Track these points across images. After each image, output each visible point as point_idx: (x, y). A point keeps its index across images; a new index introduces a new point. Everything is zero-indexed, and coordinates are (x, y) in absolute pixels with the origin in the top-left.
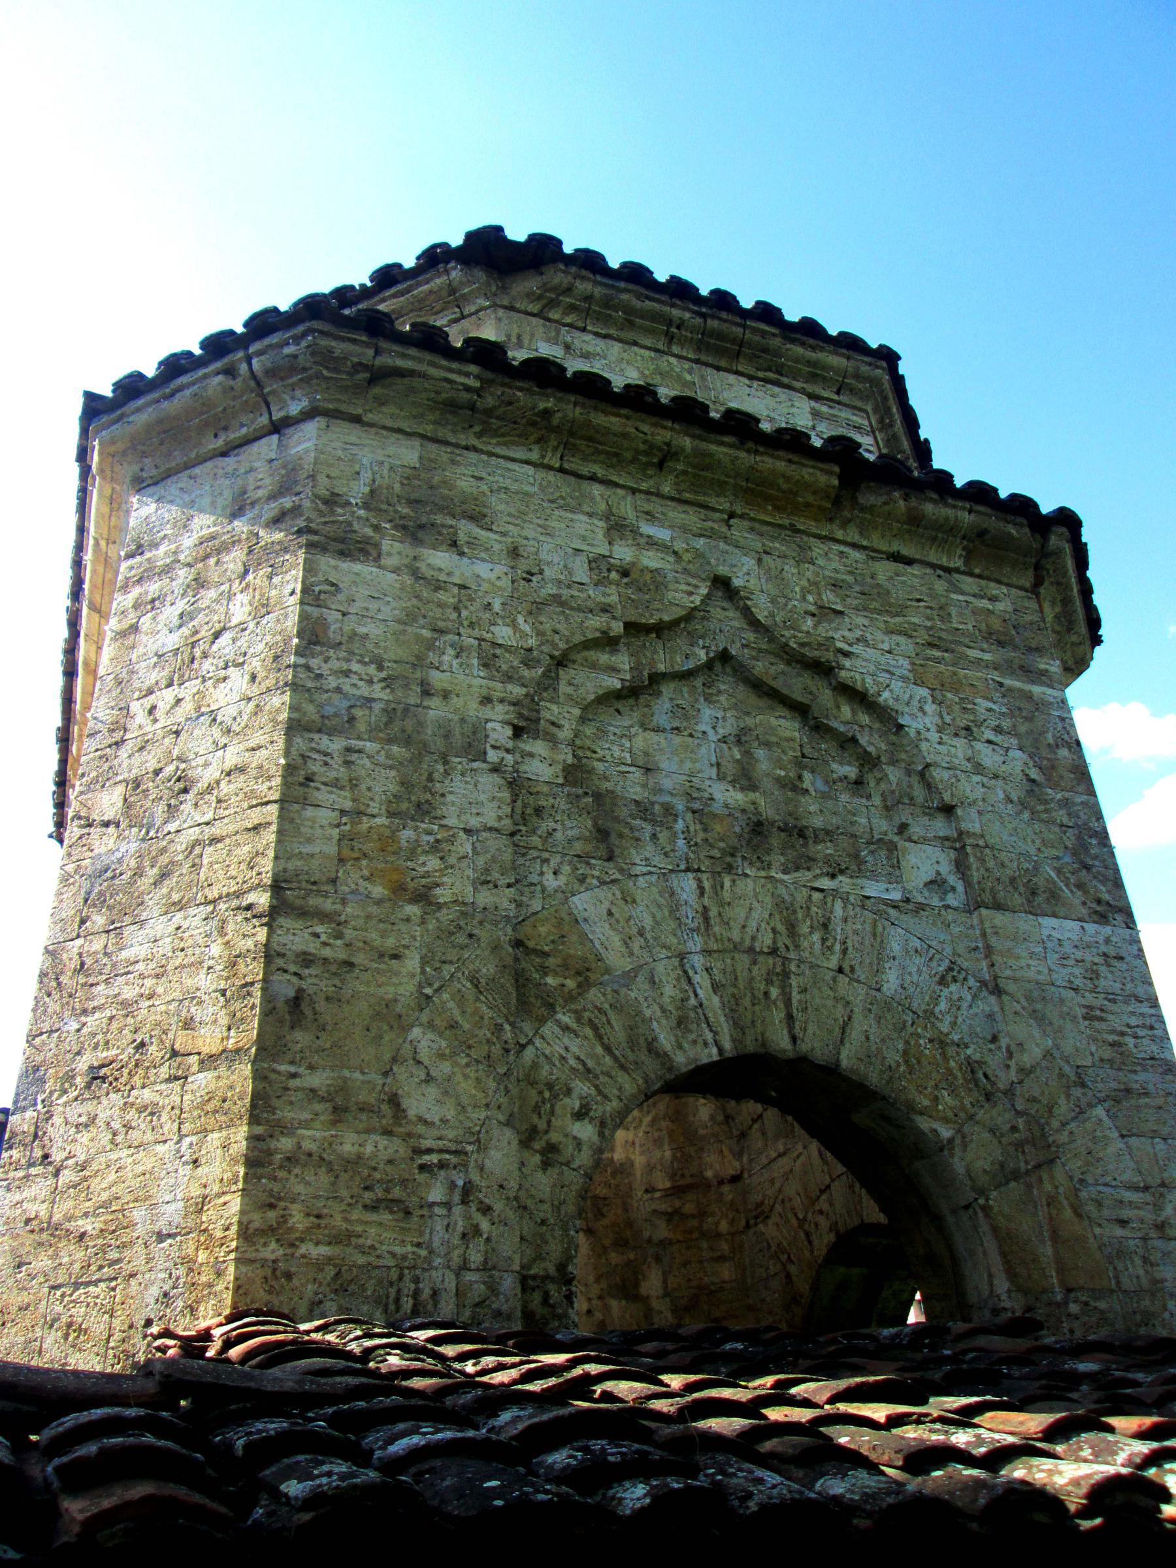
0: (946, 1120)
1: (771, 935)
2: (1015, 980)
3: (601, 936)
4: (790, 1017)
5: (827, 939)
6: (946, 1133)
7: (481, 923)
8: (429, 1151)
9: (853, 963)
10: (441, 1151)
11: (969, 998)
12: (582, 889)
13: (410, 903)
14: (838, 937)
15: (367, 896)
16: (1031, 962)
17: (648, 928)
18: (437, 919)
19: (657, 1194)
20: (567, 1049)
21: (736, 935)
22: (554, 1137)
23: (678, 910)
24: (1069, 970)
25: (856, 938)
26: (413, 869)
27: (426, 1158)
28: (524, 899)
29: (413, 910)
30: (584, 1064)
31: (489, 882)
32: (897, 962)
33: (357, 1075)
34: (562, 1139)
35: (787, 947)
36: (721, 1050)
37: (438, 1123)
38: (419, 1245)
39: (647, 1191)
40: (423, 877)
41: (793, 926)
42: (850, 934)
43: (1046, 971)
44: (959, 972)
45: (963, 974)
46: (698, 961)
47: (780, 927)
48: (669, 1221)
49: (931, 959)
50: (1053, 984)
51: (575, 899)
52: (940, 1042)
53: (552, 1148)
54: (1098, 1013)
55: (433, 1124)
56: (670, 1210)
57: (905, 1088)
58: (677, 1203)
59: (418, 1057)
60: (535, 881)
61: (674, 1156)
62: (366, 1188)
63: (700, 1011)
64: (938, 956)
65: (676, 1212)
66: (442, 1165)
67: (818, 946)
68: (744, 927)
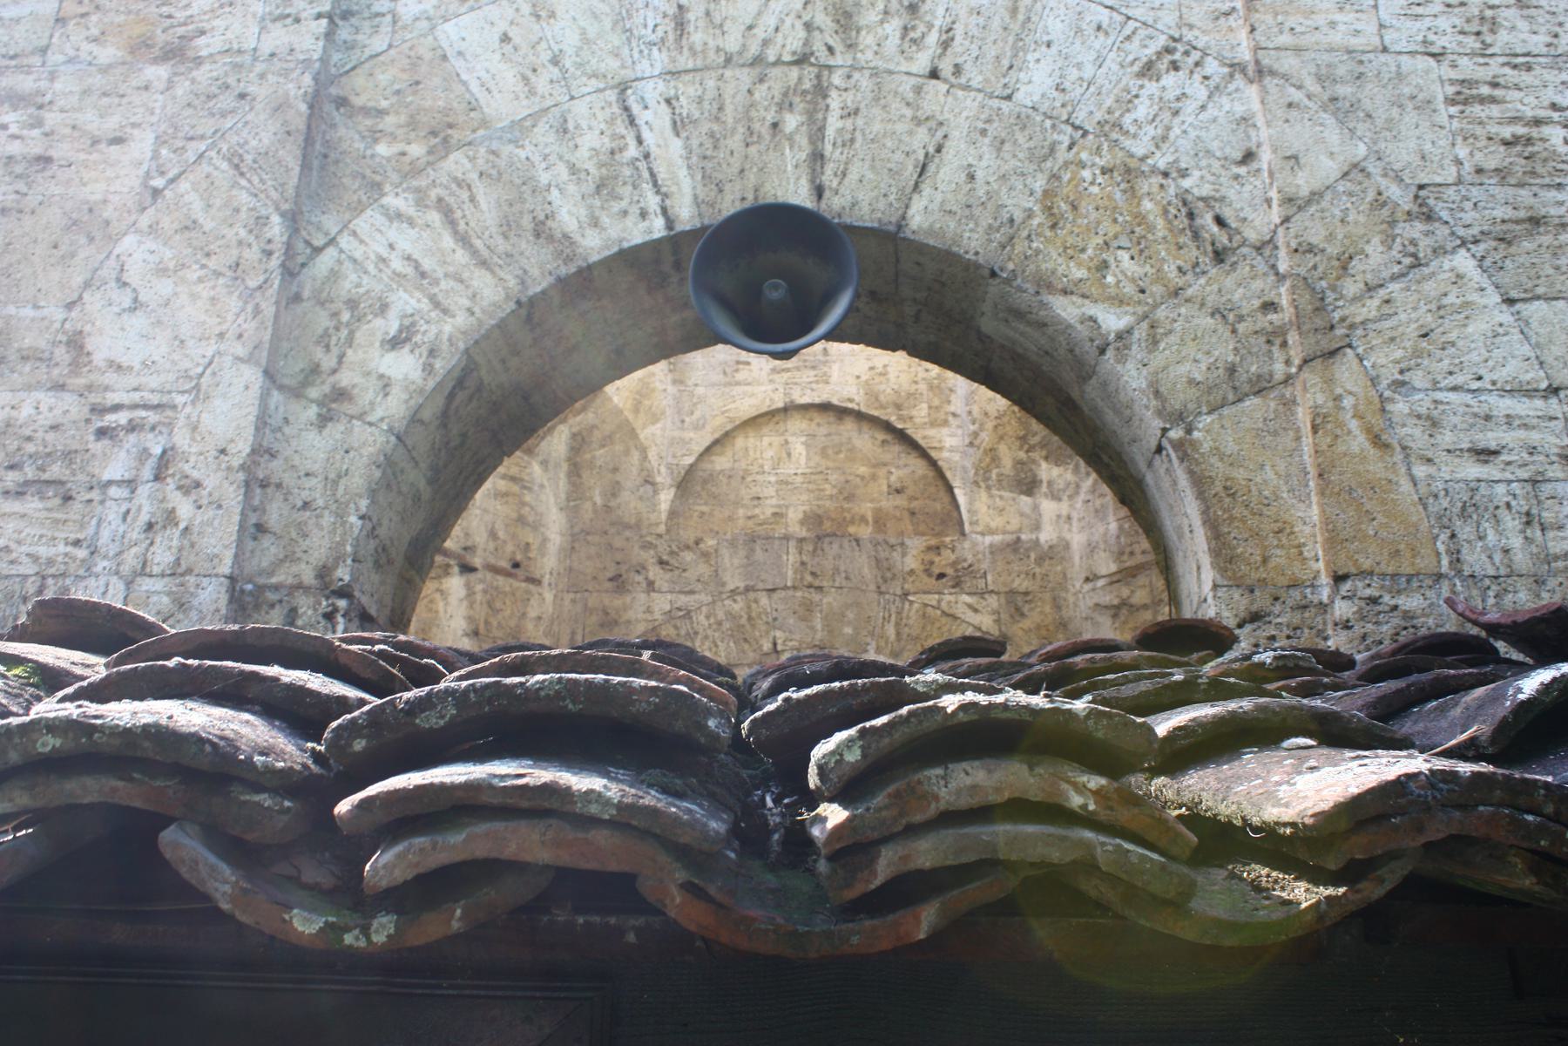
0: (1119, 301)
1: (802, 34)
2: (1298, 50)
3: (483, 74)
4: (817, 157)
5: (914, 28)
6: (1112, 321)
7: (262, 76)
8: (117, 408)
9: (960, 60)
10: (135, 407)
11: (1202, 93)
12: (463, 10)
13: (152, 64)
14: (937, 23)
15: (90, 64)
16: (1338, 17)
17: (570, 51)
18: (193, 81)
19: (1100, 583)
20: (391, 247)
21: (732, 43)
22: (345, 378)
23: (630, 17)
24: (1427, 22)
25: (974, 19)
26: (170, 17)
27: (110, 419)
28: (360, 37)
29: (157, 73)
30: (417, 266)
31: (288, 16)
32: (1054, 49)
33: (28, 312)
34: (358, 380)
35: (830, 50)
36: (670, 224)
37: (137, 367)
38: (77, 543)
39: (1087, 580)
40: (185, 24)
41: (848, 15)
42: (963, 13)
43: (1372, 28)
44: (1187, 53)
45: (1196, 56)
46: (653, 90)
47: (822, 19)
48: (1115, 616)
49: (1128, 38)
50: (1385, 50)
51: (449, 27)
52: (1129, 173)
53: (341, 395)
54: (1485, 90)
55: (131, 368)
56: (1116, 602)
57: (1038, 252)
58: (1125, 592)
59: (125, 277)
60: (384, 10)
61: (1121, 528)
62: (11, 467)
63: (642, 165)
64: (1142, 32)
65: (1124, 603)
66: (132, 427)
67: (894, 41)
68: (750, 28)
